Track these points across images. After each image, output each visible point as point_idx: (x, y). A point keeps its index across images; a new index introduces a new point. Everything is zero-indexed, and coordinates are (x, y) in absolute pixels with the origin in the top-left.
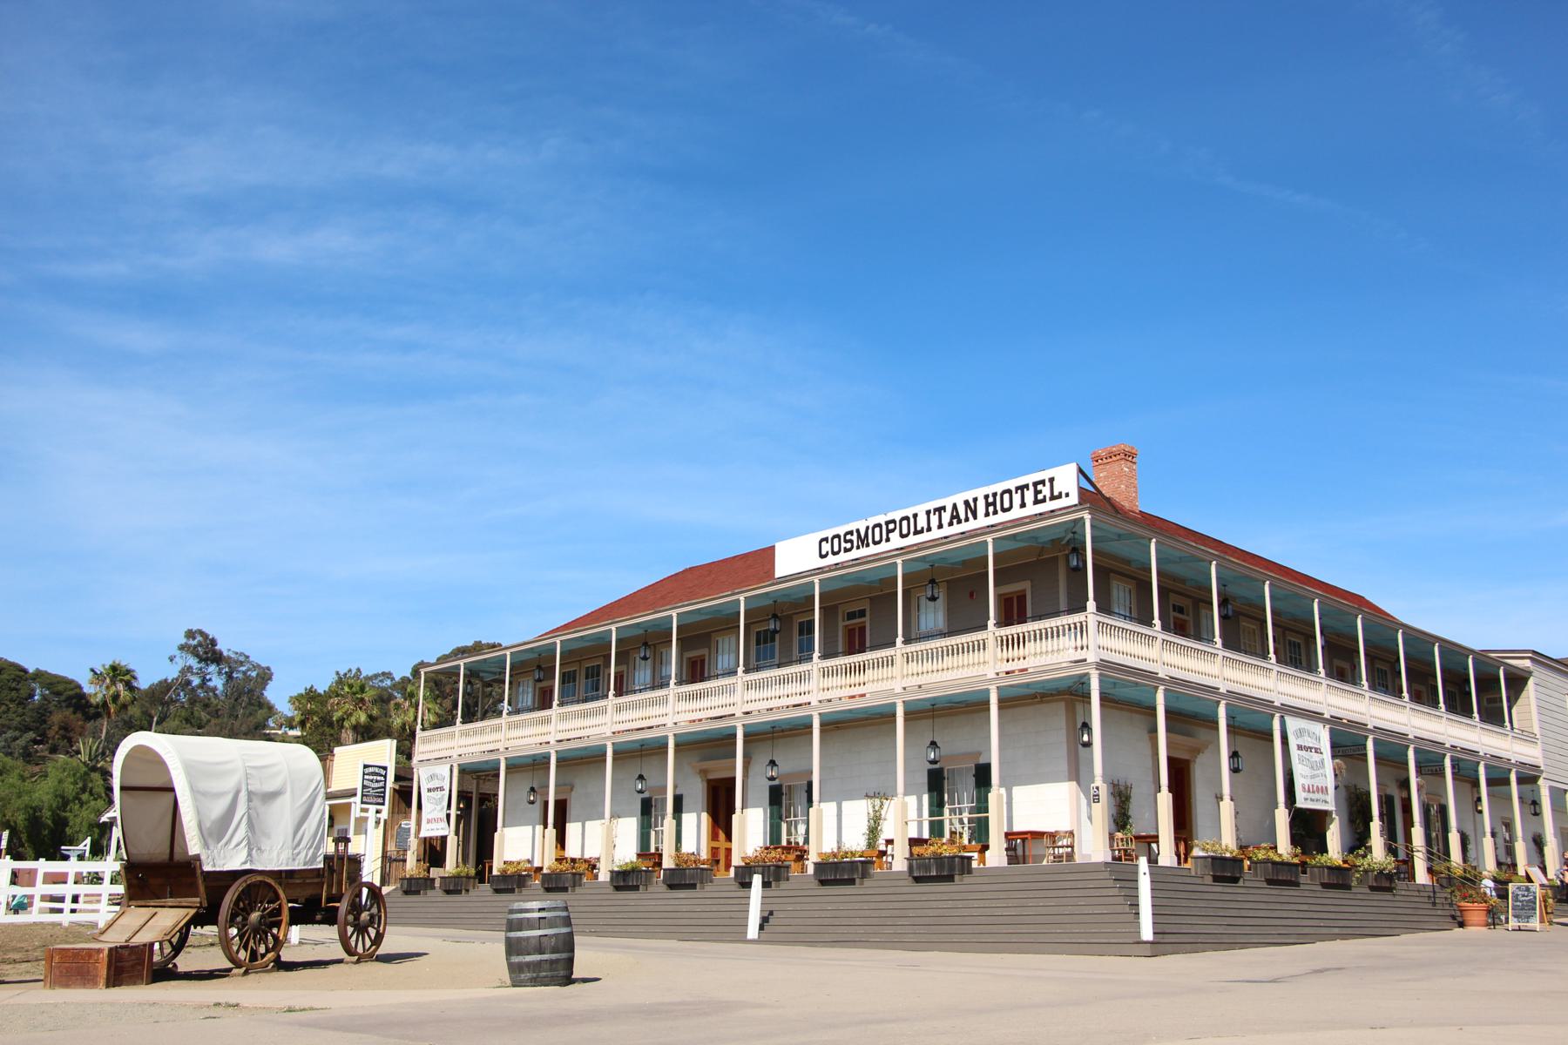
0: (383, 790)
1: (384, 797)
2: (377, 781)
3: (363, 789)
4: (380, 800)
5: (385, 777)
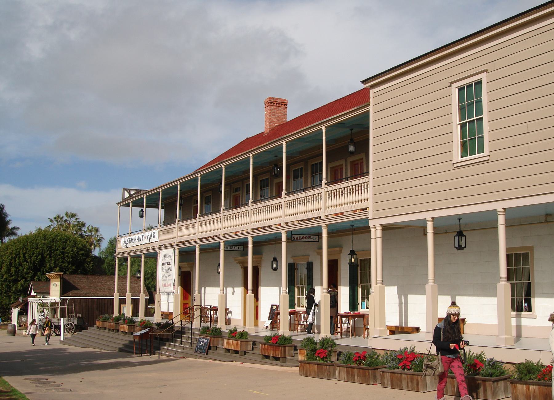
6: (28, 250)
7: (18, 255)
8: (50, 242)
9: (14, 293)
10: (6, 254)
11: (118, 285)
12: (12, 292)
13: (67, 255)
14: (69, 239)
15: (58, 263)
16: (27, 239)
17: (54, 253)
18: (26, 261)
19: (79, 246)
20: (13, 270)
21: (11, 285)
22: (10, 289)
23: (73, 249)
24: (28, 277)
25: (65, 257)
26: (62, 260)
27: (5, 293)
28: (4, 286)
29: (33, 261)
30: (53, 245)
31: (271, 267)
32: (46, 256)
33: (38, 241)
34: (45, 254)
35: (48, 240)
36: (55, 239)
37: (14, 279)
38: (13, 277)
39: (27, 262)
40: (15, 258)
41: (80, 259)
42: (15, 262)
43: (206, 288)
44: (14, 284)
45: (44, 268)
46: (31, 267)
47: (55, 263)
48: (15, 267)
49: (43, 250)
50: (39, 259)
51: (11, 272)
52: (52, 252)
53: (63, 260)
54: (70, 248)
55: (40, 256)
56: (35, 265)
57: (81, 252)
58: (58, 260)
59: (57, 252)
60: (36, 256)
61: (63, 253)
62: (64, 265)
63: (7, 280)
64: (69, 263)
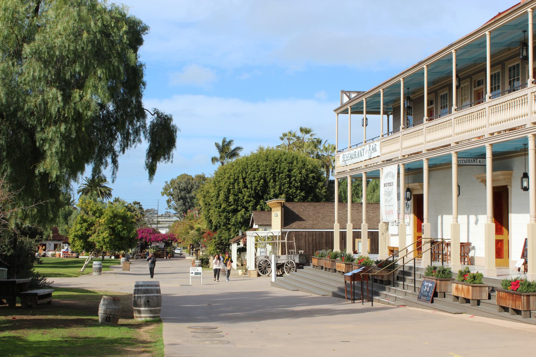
7: (236, 180)
8: (274, 163)
9: (234, 225)
10: (223, 179)
11: (339, 213)
12: (231, 224)
13: (294, 178)
14: (297, 159)
15: (284, 188)
16: (247, 160)
17: (278, 176)
18: (246, 187)
19: (309, 167)
20: (231, 198)
21: (229, 216)
22: (229, 221)
23: (301, 171)
24: (249, 206)
25: (292, 182)
26: (289, 184)
27: (224, 226)
28: (222, 217)
29: (254, 186)
30: (277, 167)
31: (520, 187)
32: (270, 181)
34: (268, 178)
36: (279, 159)
37: (233, 208)
38: (232, 207)
39: (248, 188)
40: (233, 184)
41: (311, 183)
42: (234, 188)
43: (444, 216)
44: (234, 215)
45: (267, 195)
46: (253, 194)
47: (280, 188)
48: (234, 195)
49: (266, 173)
50: (261, 185)
51: (230, 201)
53: (289, 185)
54: (298, 170)
55: (262, 180)
56: (257, 191)
57: (311, 175)
58: (284, 185)
59: (282, 176)
60: (257, 181)
61: (289, 176)
62: (291, 191)
63: (226, 211)
64: (297, 188)
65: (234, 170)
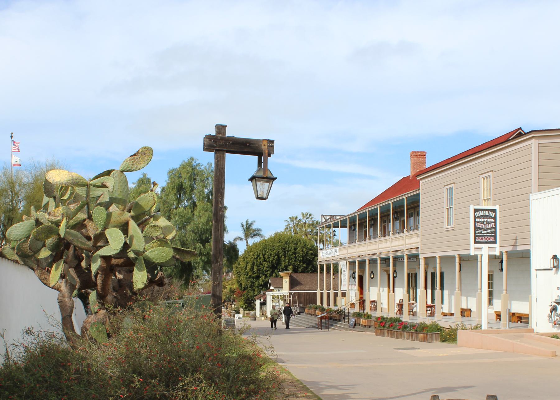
0: (494, 230)
1: (495, 237)
2: (488, 223)
3: (475, 230)
4: (492, 240)
5: (495, 218)
6: (267, 252)
9: (257, 287)
13: (298, 255)
14: (300, 241)
15: (291, 262)
16: (266, 242)
18: (265, 261)
19: (308, 247)
20: (255, 268)
22: (254, 284)
24: (268, 274)
27: (250, 287)
28: (249, 282)
30: (286, 247)
32: (282, 257)
33: (274, 244)
35: (282, 243)
36: (288, 241)
38: (256, 274)
40: (257, 259)
41: (310, 257)
42: (257, 262)
47: (289, 261)
48: (257, 266)
51: (254, 270)
52: (286, 253)
55: (276, 256)
57: (310, 252)
58: (291, 259)
61: (295, 253)
62: (296, 263)
64: (300, 261)
65: (257, 250)
